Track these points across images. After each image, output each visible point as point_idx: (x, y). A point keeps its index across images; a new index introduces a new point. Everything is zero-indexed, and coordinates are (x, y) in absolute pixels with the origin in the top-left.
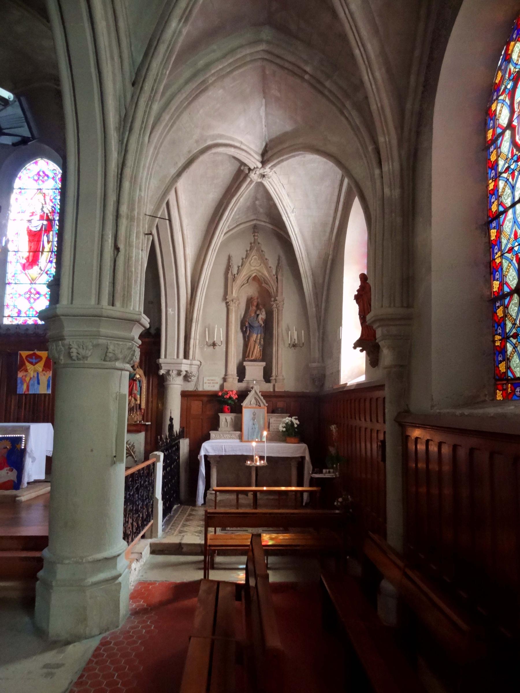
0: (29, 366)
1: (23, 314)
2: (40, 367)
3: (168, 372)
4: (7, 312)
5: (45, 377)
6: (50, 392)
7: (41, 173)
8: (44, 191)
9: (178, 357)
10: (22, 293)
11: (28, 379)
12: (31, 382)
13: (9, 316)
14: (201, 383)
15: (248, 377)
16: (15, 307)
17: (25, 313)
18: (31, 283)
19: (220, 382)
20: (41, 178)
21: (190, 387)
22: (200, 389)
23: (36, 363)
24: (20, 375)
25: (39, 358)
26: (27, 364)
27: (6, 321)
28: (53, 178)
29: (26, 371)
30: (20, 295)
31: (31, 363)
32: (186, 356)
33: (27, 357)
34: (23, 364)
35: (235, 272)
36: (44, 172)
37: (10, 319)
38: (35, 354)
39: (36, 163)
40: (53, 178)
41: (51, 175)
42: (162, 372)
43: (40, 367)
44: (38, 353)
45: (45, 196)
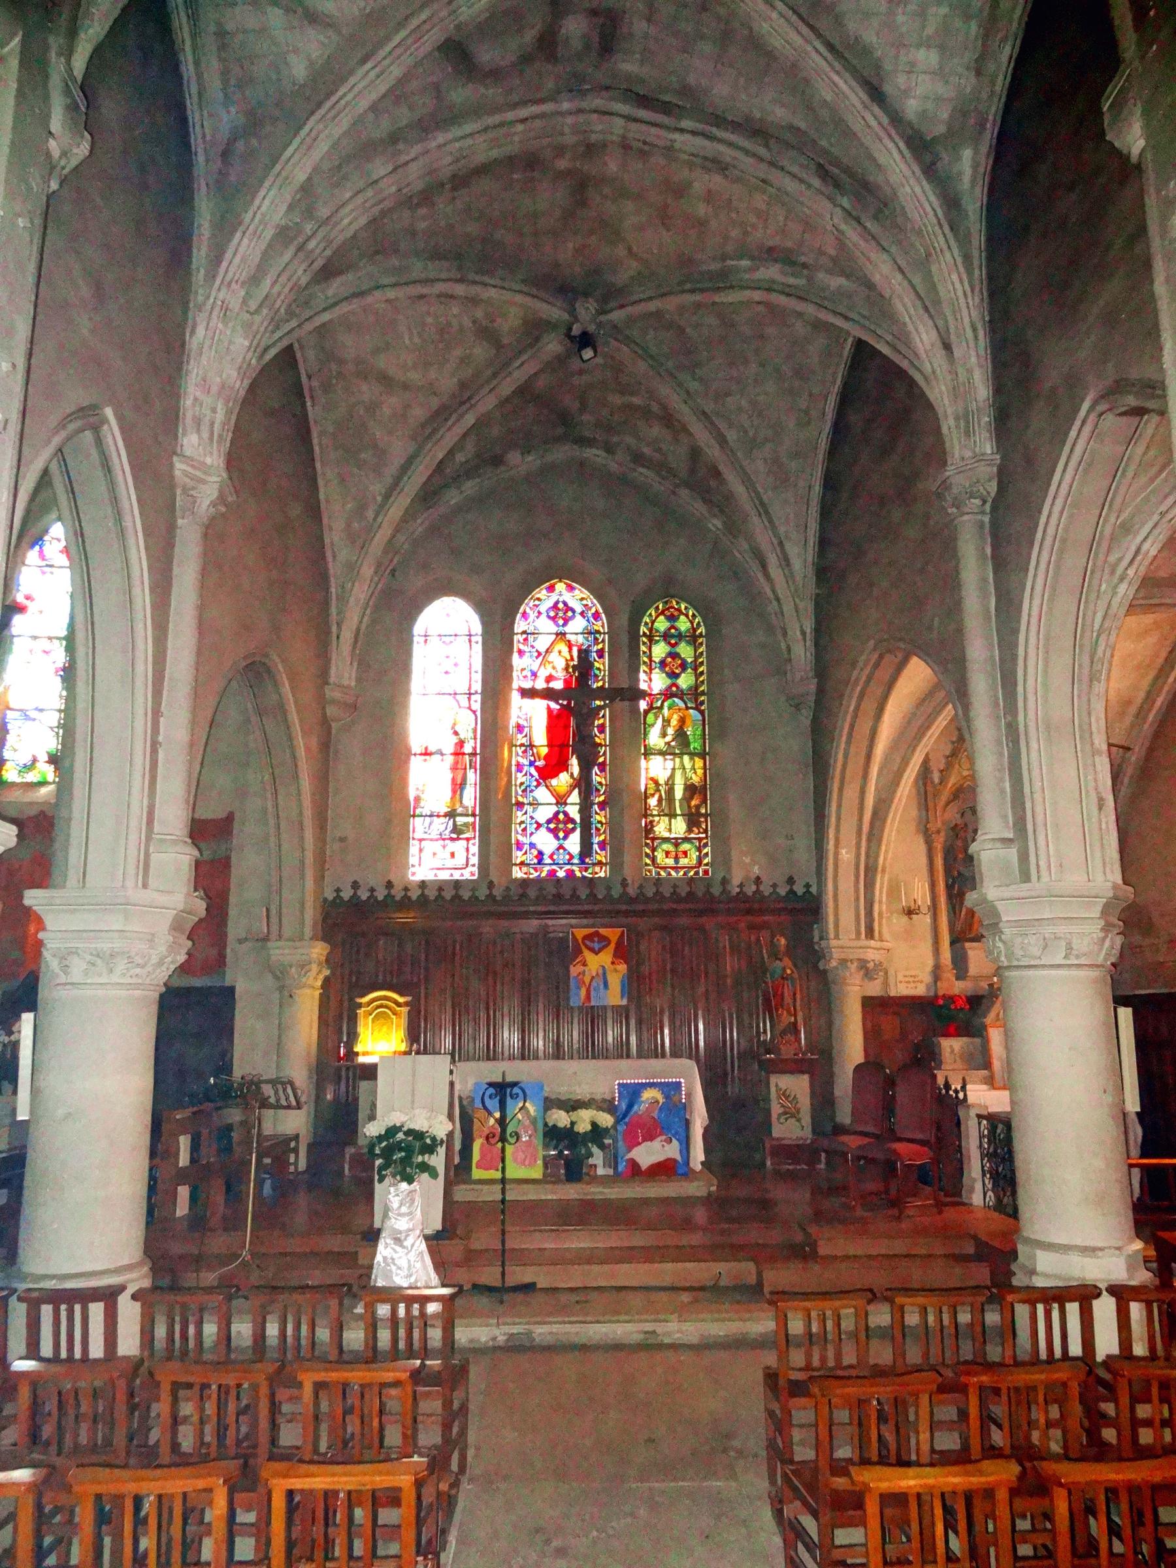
0: (587, 954)
1: (547, 860)
2: (606, 958)
3: (844, 962)
4: (518, 856)
5: (617, 975)
6: (624, 1002)
7: (561, 606)
8: (568, 637)
9: (858, 933)
10: (542, 820)
11: (587, 980)
12: (594, 984)
13: (522, 863)
14: (891, 981)
15: (973, 970)
16: (532, 846)
17: (551, 857)
18: (557, 803)
19: (928, 979)
20: (561, 614)
21: (874, 989)
22: (892, 994)
23: (600, 950)
24: (574, 970)
25: (605, 940)
26: (586, 953)
27: (518, 873)
28: (582, 614)
29: (585, 964)
30: (539, 826)
31: (592, 950)
32: (870, 933)
33: (586, 937)
34: (578, 952)
35: (937, 781)
36: (565, 604)
37: (525, 869)
38: (597, 934)
39: (551, 589)
40: (582, 614)
41: (579, 608)
42: (834, 963)
43: (606, 958)
44: (602, 931)
45: (570, 647)
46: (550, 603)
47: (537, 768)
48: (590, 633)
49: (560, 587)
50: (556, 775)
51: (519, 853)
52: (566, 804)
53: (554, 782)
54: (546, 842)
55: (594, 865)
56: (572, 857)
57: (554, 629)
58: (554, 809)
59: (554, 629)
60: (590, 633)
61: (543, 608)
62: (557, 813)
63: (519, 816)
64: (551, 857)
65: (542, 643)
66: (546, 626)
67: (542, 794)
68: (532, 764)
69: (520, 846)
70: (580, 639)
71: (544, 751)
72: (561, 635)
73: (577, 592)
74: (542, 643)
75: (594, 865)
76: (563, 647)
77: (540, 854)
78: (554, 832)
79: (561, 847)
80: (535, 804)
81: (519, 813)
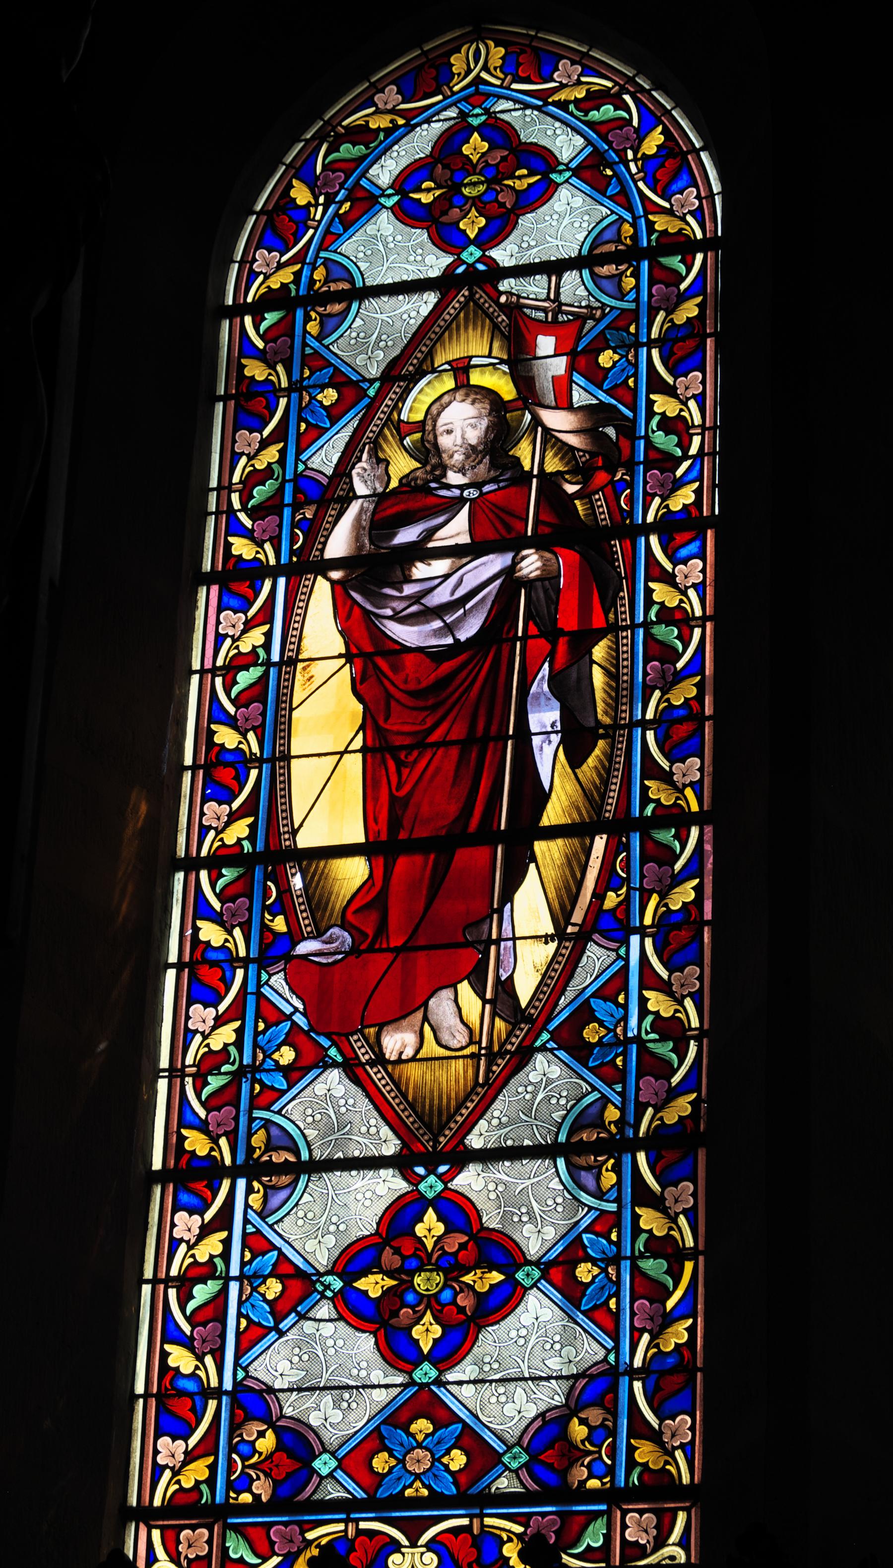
10: (321, 1253)
16: (252, 1401)
41: (567, 146)
46: (420, 142)
47: (302, 975)
48: (631, 255)
49: (477, 62)
50: (410, 1004)
51: (170, 1449)
52: (462, 1157)
53: (397, 1042)
54: (329, 1375)
55: (615, 1497)
56: (483, 1456)
57: (436, 263)
58: (389, 1185)
59: (436, 263)
60: (631, 255)
61: (385, 172)
62: (401, 1215)
63: (181, 1233)
64: (356, 1460)
65: (371, 335)
66: (390, 249)
67: (326, 1104)
68: (273, 952)
69: (176, 1407)
70: (574, 287)
71: (352, 873)
72: (467, 291)
73: (565, 71)
74: (371, 335)
75: (615, 1497)
76: (475, 344)
77: (298, 1443)
78: (380, 1321)
79: (425, 1402)
80: (286, 1167)
81: (186, 1224)
